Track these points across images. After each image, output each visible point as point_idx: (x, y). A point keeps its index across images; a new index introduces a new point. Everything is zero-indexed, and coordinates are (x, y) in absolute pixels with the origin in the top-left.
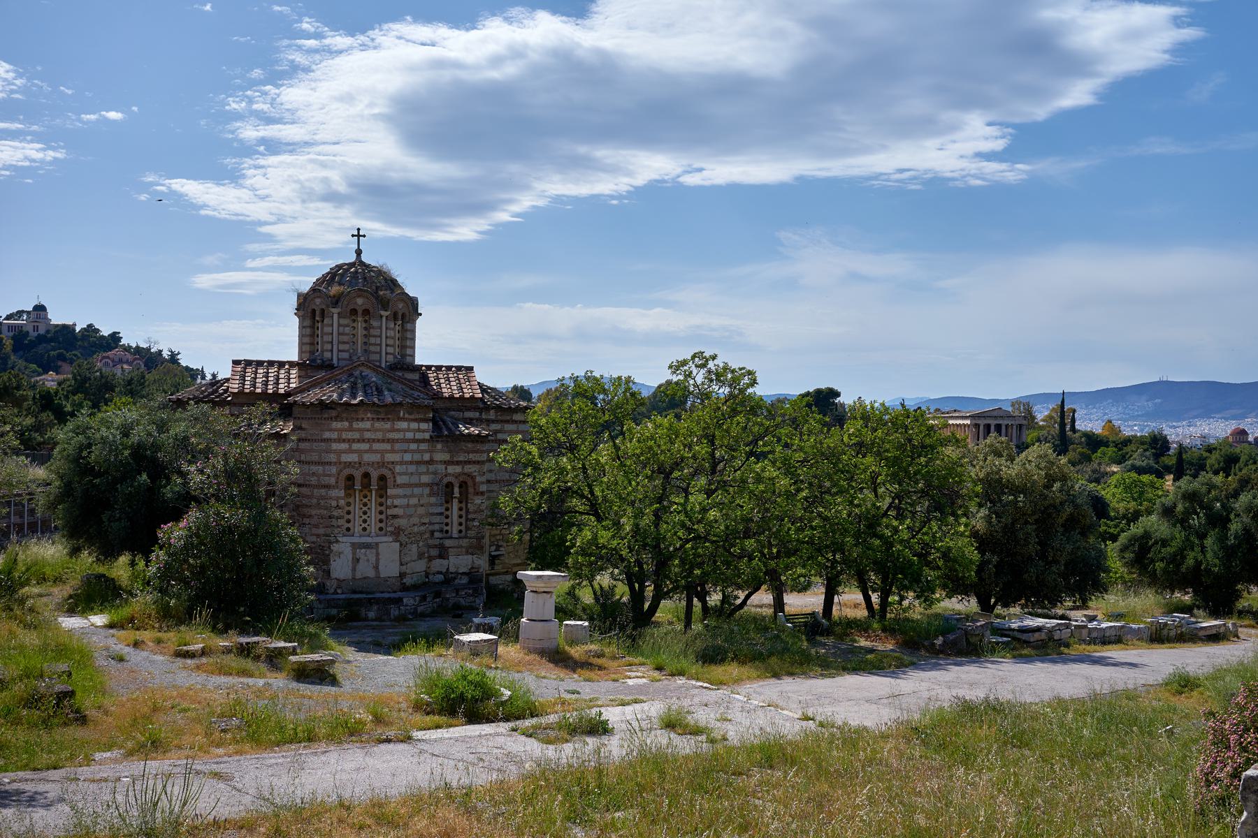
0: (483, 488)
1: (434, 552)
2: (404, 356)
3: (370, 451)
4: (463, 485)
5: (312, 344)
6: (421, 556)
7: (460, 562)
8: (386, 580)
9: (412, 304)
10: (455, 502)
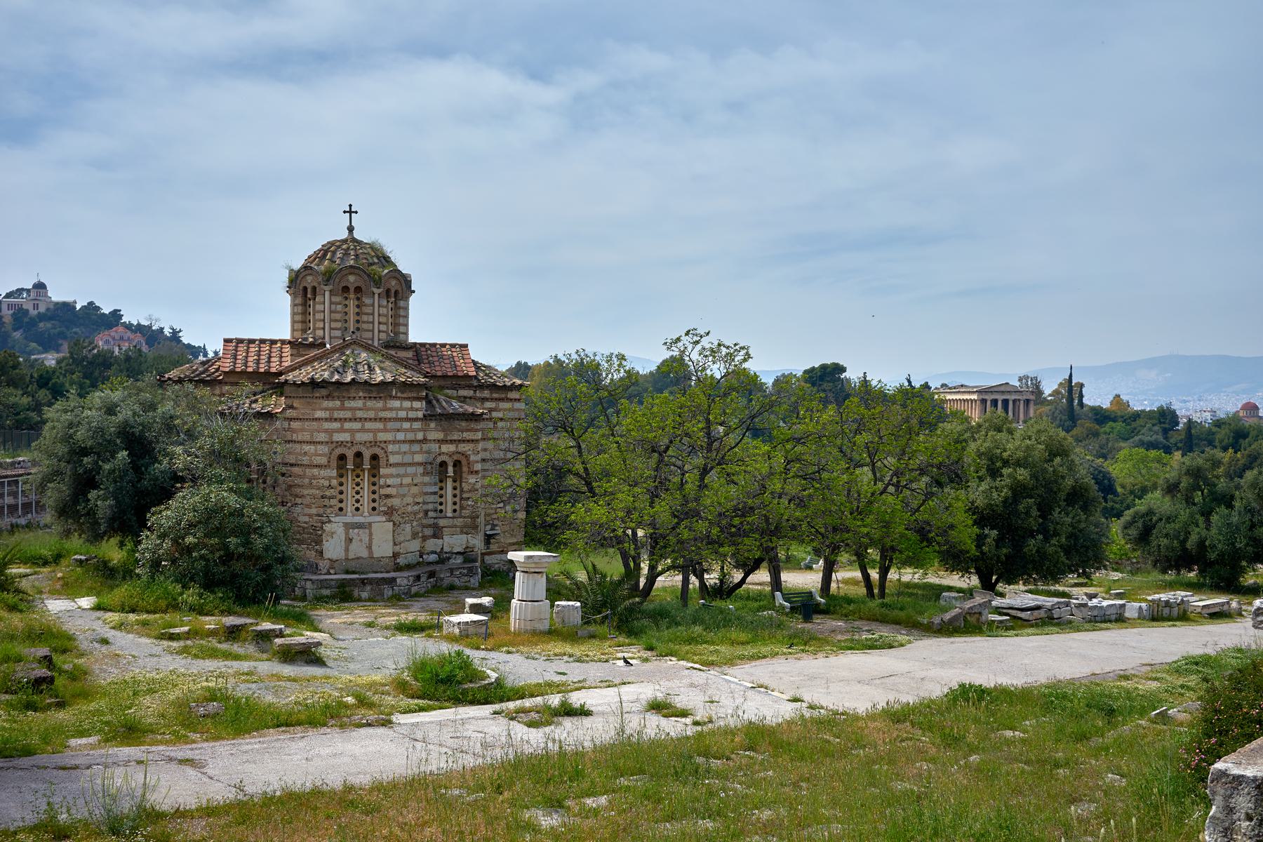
0: (478, 467)
1: (428, 532)
3: (363, 430)
4: (457, 464)
5: (303, 322)
6: (415, 535)
7: (454, 542)
8: (379, 559)
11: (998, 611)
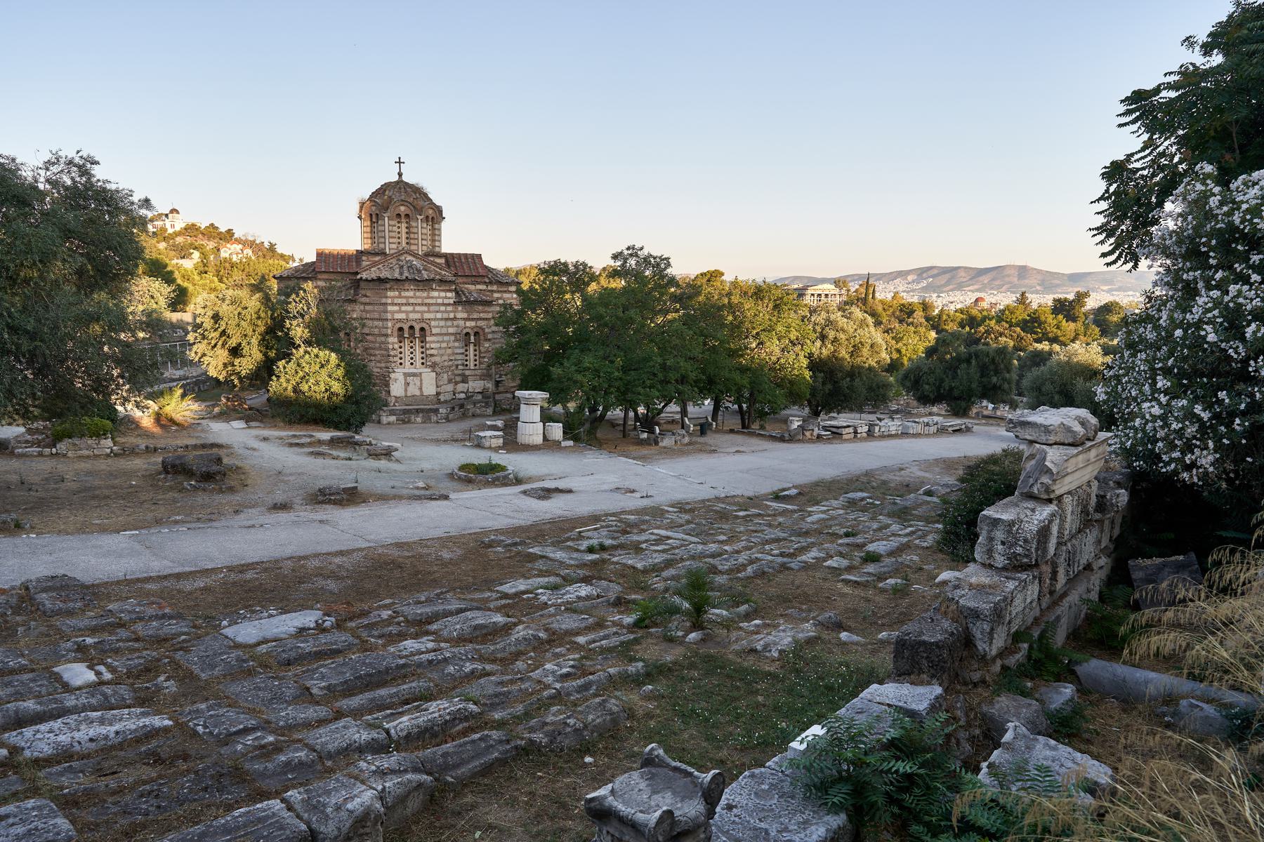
0: (490, 336)
1: (458, 379)
2: (434, 247)
3: (414, 311)
4: (476, 334)
6: (450, 381)
7: (475, 385)
8: (427, 397)
9: (439, 210)
11: (825, 428)
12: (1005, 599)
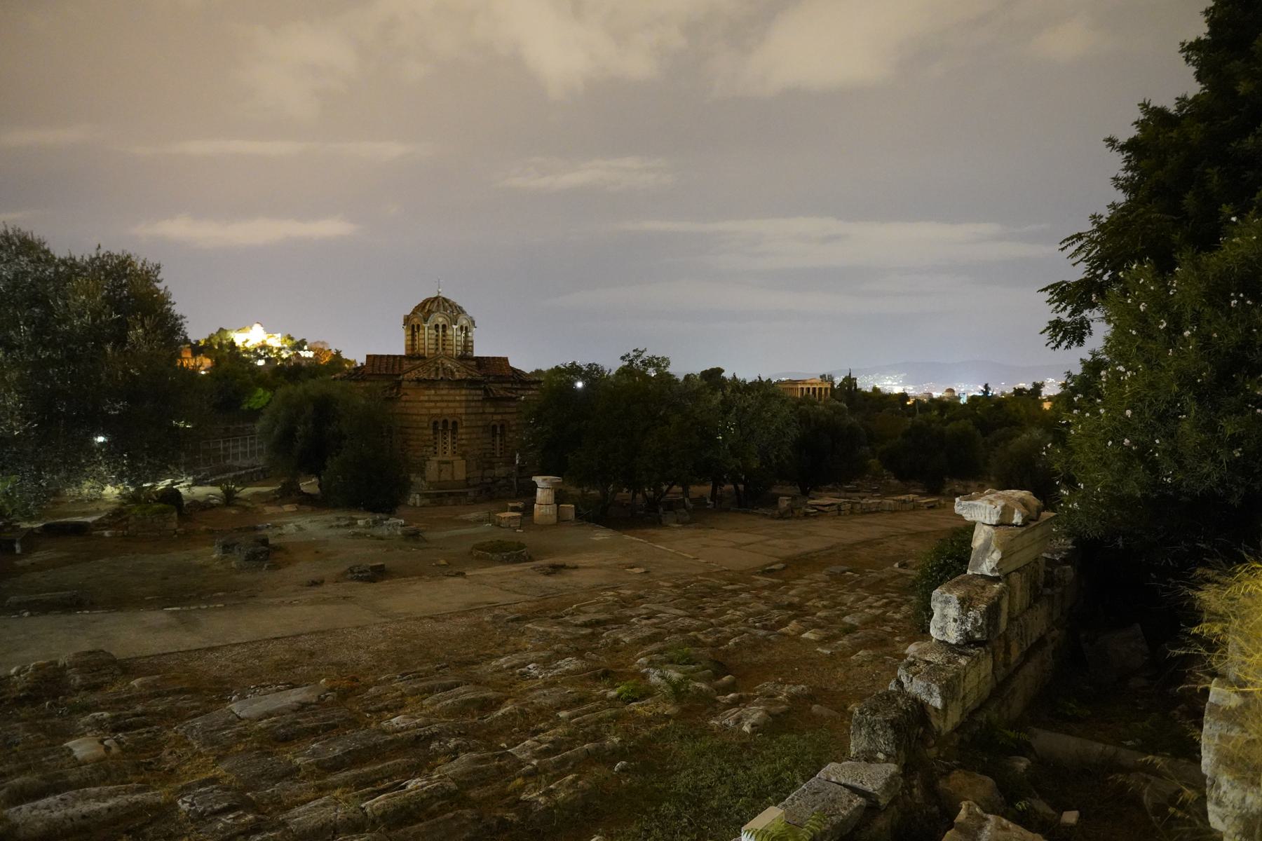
3: (448, 407)
4: (502, 426)
7: (500, 471)
10: (498, 438)
11: (812, 506)
12: (958, 676)
